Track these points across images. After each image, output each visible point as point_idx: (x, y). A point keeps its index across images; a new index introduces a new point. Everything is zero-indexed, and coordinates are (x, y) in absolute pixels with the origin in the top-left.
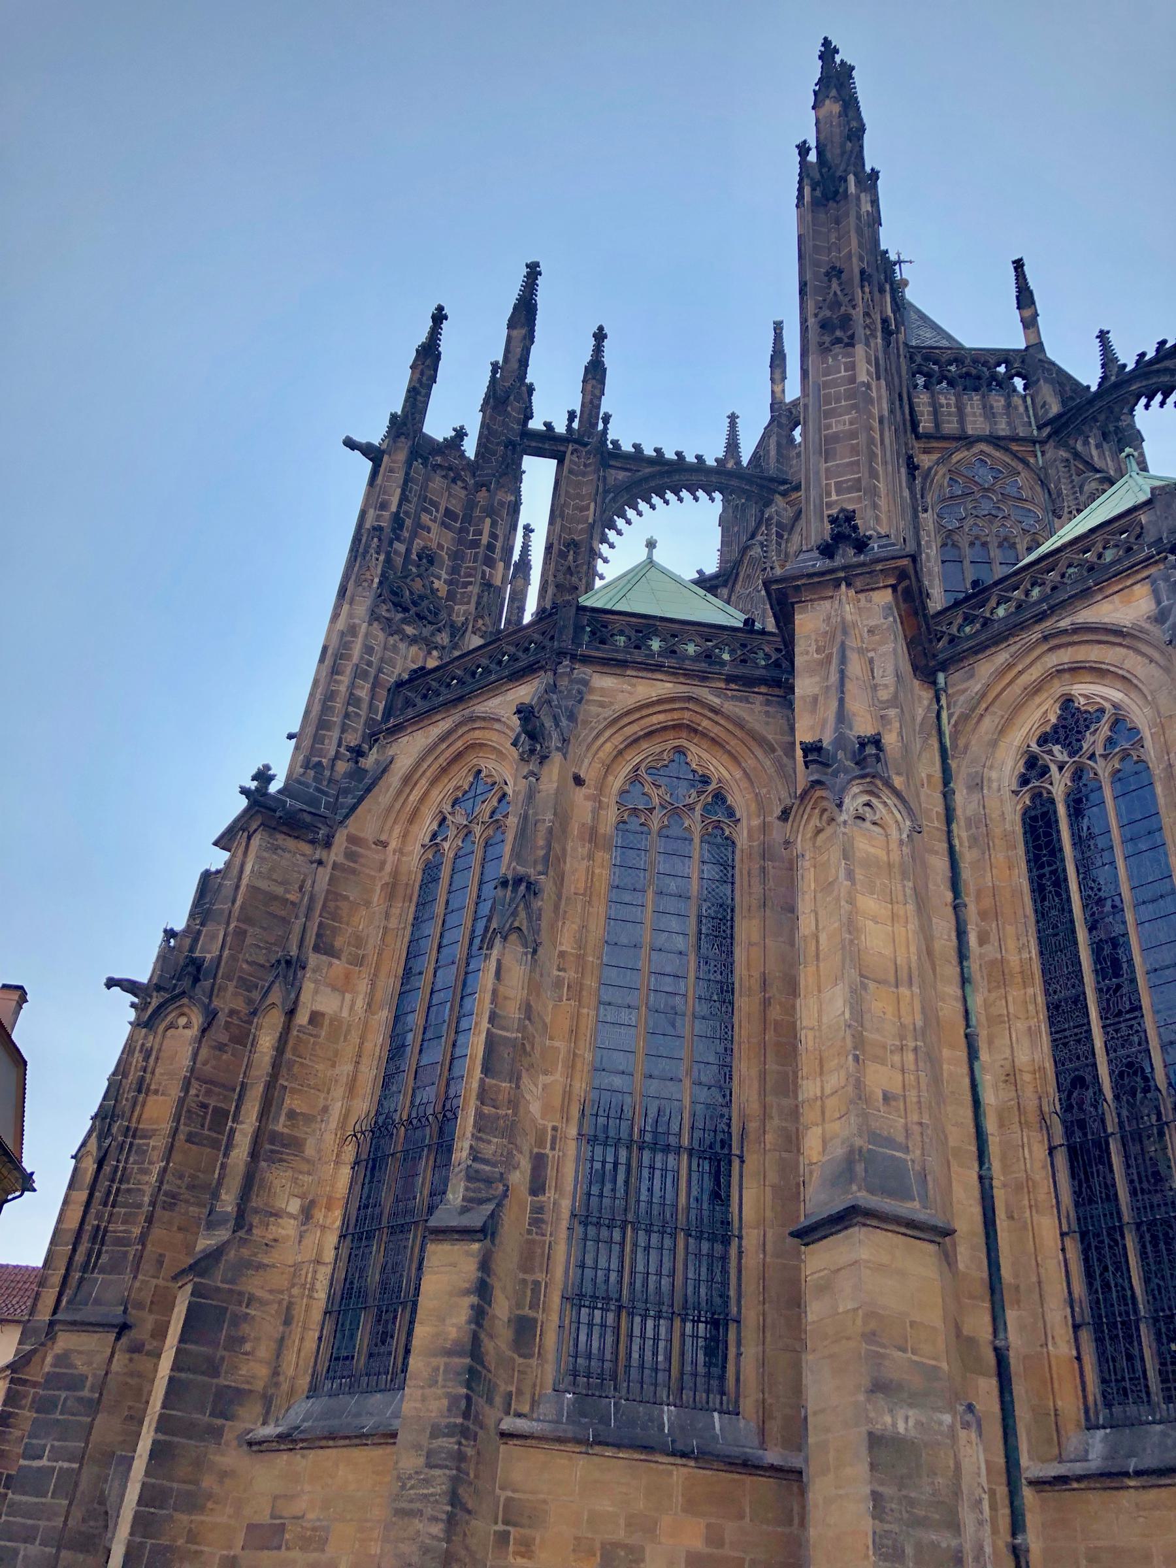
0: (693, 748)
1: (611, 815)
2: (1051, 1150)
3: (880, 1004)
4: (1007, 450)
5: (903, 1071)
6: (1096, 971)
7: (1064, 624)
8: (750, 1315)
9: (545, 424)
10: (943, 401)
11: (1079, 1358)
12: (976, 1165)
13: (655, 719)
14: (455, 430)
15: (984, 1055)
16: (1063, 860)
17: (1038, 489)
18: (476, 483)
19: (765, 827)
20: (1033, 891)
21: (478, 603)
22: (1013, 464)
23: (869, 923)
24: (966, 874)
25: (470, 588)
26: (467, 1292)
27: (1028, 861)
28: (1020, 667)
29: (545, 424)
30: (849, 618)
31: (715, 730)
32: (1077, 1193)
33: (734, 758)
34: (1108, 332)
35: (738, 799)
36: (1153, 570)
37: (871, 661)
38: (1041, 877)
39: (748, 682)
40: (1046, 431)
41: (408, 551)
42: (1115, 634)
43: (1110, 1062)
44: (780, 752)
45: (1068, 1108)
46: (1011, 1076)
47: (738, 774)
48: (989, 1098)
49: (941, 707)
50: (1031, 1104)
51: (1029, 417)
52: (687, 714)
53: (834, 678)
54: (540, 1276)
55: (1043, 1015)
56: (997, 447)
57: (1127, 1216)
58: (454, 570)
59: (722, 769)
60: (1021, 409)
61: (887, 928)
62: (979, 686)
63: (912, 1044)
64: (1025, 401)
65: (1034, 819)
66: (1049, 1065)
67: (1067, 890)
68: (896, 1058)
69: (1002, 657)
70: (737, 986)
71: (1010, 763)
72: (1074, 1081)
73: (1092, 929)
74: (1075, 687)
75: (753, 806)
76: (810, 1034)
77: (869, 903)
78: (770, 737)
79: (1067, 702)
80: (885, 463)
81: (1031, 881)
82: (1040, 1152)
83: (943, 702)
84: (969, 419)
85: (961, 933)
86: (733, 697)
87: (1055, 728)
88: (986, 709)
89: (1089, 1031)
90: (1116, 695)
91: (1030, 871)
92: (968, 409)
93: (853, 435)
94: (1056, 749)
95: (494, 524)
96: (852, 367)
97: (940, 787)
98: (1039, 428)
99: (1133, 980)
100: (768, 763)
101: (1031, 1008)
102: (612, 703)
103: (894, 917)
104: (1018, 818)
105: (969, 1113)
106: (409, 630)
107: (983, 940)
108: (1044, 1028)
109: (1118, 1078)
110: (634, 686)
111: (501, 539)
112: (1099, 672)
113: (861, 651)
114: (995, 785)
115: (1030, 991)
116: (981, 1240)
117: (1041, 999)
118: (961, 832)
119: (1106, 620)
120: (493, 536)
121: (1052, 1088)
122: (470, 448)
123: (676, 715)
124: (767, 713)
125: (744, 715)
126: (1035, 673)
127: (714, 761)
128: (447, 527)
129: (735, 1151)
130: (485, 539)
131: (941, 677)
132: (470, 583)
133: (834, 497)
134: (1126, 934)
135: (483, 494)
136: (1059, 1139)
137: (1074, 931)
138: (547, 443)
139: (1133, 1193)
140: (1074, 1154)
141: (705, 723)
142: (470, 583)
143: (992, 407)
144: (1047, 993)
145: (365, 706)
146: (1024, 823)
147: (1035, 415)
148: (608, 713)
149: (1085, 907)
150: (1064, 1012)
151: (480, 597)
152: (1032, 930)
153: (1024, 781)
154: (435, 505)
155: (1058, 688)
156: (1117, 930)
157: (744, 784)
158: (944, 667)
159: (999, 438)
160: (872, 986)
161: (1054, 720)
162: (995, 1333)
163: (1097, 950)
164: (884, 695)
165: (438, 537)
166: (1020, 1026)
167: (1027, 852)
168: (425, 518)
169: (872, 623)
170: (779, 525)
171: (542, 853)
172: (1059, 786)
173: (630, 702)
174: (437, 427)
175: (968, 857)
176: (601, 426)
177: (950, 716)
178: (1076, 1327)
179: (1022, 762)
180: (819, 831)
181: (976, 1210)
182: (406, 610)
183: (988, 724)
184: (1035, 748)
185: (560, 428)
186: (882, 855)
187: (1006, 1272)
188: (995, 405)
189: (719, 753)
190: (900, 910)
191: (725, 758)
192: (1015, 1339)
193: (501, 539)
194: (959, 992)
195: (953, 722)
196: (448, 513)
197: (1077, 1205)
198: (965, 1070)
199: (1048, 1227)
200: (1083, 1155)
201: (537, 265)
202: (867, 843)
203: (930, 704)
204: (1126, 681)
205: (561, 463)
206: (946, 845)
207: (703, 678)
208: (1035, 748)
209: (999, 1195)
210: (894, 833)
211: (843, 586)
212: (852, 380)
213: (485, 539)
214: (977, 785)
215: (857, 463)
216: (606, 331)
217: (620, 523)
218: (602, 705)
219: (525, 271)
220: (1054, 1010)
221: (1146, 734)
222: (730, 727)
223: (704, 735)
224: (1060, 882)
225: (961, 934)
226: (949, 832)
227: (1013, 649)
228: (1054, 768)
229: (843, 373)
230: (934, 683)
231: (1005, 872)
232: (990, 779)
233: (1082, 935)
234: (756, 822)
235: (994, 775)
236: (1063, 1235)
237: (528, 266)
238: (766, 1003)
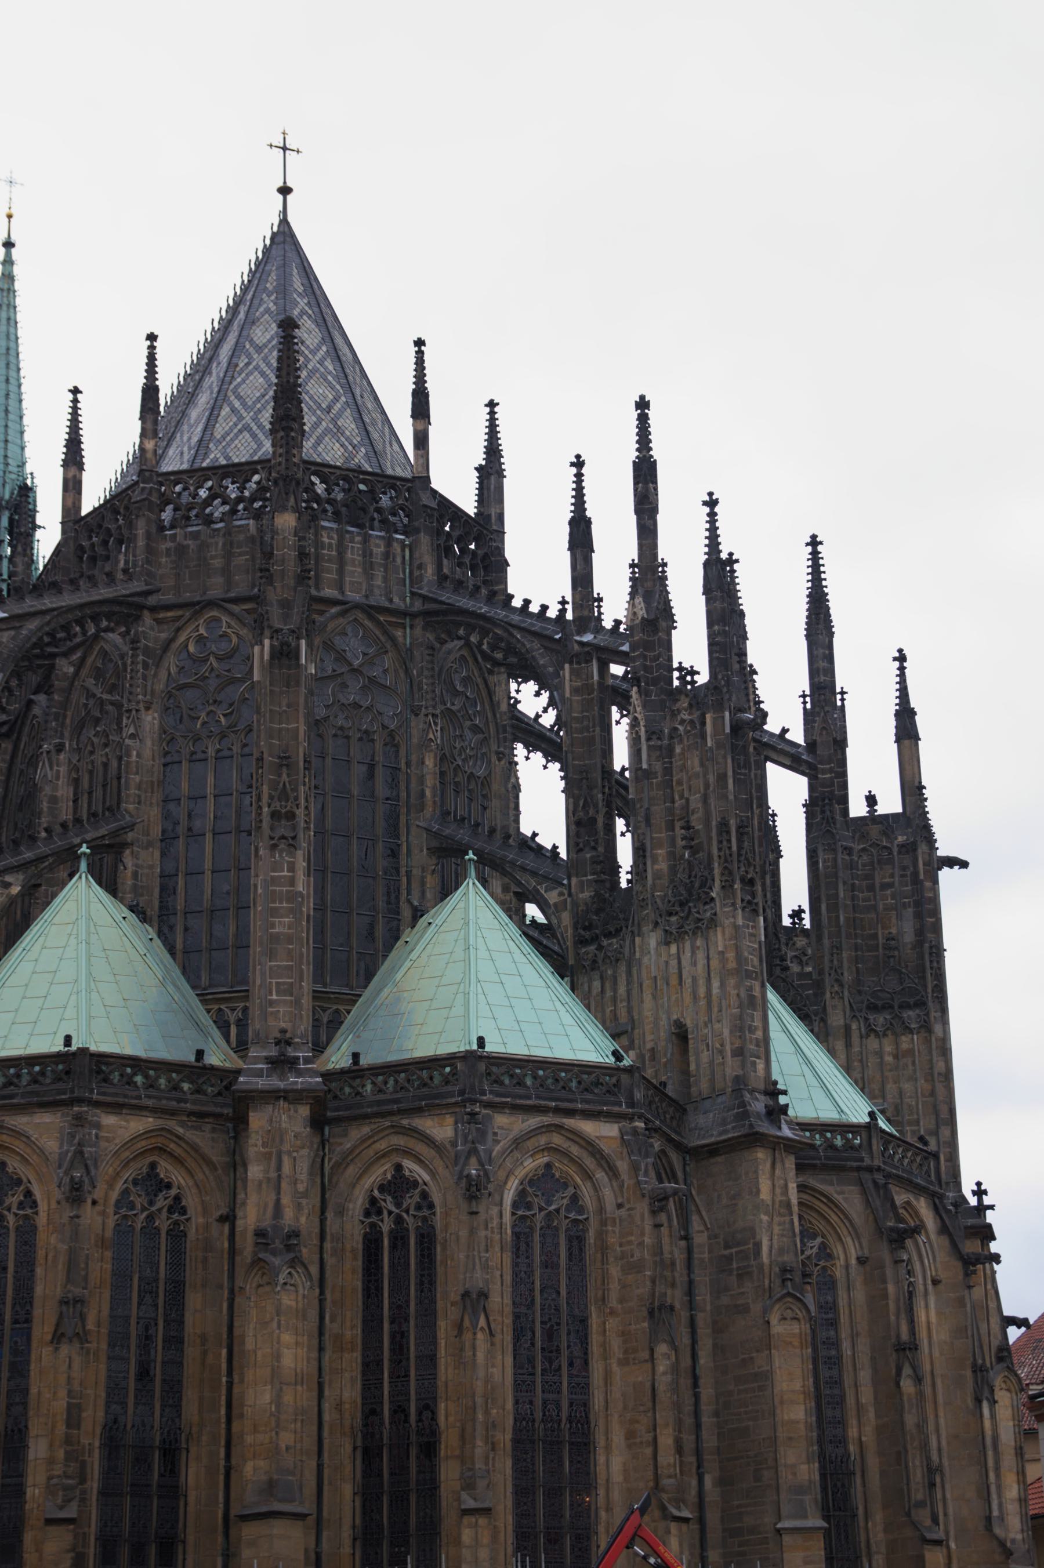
0: (163, 1163)
1: (111, 1222)
2: (355, 1449)
3: (288, 1398)
4: (379, 623)
5: (295, 1432)
6: (391, 1350)
7: (405, 1122)
8: (191, 1539)
10: (326, 540)
11: (354, 1554)
12: (316, 1457)
13: (139, 1145)
15: (327, 1393)
16: (382, 1274)
17: (402, 675)
19: (207, 1227)
20: (364, 1290)
22: (382, 638)
23: (285, 1350)
24: (328, 1273)
26: (68, 1551)
27: (364, 1269)
28: (376, 1138)
30: (284, 1125)
31: (178, 1151)
32: (364, 1472)
34: (498, 404)
35: (191, 1201)
36: (457, 1110)
37: (295, 1158)
38: (369, 1281)
39: (201, 1115)
40: (418, 605)
42: (429, 1141)
43: (390, 1402)
44: (220, 1171)
45: (365, 1425)
46: (339, 1406)
47: (191, 1183)
48: (326, 1417)
49: (325, 1154)
50: (347, 1422)
51: (404, 573)
52: (160, 1139)
53: (273, 1175)
54: (86, 1530)
55: (360, 1368)
56: (371, 617)
57: (386, 1488)
59: (180, 1178)
60: (399, 560)
61: (293, 1353)
62: (349, 1146)
63: (300, 1418)
64: (403, 551)
66: (359, 1400)
67: (382, 1295)
68: (293, 1426)
69: (366, 1130)
70: (186, 1339)
71: (360, 1202)
72: (371, 1412)
73: (392, 1322)
74: (405, 1161)
75: (199, 1208)
76: (250, 1410)
77: (287, 1338)
78: (214, 1159)
79: (399, 1168)
80: (308, 964)
81: (363, 1283)
82: (348, 1448)
83: (327, 1150)
84: (349, 568)
85: (322, 1318)
86: (192, 1126)
87: (389, 1182)
88: (352, 1160)
89: (382, 1383)
90: (426, 1177)
91: (364, 1276)
92: (349, 555)
93: (289, 939)
94: (389, 1199)
96: (292, 868)
97: (319, 1213)
98: (413, 594)
99: (408, 1359)
100: (211, 1178)
101: (354, 1365)
102: (114, 1138)
103: (297, 1343)
104: (361, 1239)
105: (315, 1428)
107: (332, 1321)
108: (359, 1377)
109: (394, 1412)
110: (127, 1121)
112: (419, 1161)
113: (289, 1153)
114: (350, 1213)
115: (355, 1354)
116: (314, 1498)
117: (359, 1360)
118: (328, 1245)
119: (428, 1131)
121: (359, 1415)
123: (153, 1140)
124: (213, 1139)
125: (198, 1141)
126: (382, 1145)
127: (176, 1172)
129: (184, 1445)
131: (327, 1129)
133: (274, 997)
134: (408, 1331)
136: (359, 1443)
137: (382, 1322)
139: (391, 1474)
140: (366, 1451)
141: (172, 1146)
143: (371, 555)
144: (363, 1355)
146: (364, 1243)
147: (411, 573)
148: (113, 1148)
149: (390, 1308)
150: (370, 1368)
152: (360, 1315)
153: (367, 1214)
155: (396, 1159)
156: (404, 1329)
157: (194, 1191)
158: (330, 1122)
159: (371, 607)
160: (284, 1387)
161: (389, 1176)
162: (317, 1545)
163: (393, 1337)
164: (301, 1188)
166: (347, 1375)
167: (363, 1262)
169: (297, 1129)
171: (83, 1273)
172: (386, 1226)
173: (127, 1135)
175: (330, 1261)
177: (330, 1159)
178: (355, 1539)
180: (259, 1286)
181: (313, 1483)
183: (351, 1171)
184: (376, 1193)
186: (294, 1304)
187: (325, 1514)
188: (375, 550)
190: (300, 1339)
192: (325, 1546)
194: (317, 1355)
195: (331, 1164)
197: (363, 1477)
198: (315, 1403)
199: (348, 1490)
200: (369, 1453)
202: (288, 1300)
203: (318, 1150)
204: (433, 1174)
206: (318, 1256)
207: (172, 1113)
208: (376, 1193)
209: (326, 1472)
210: (301, 1291)
211: (282, 1102)
212: (292, 882)
214: (341, 1212)
215: (290, 968)
218: (108, 1140)
220: (366, 1365)
221: (438, 1210)
222: (189, 1149)
223: (171, 1155)
224: (379, 1289)
225: (322, 1318)
226: (321, 1248)
227: (373, 1127)
228: (385, 1213)
229: (285, 873)
230: (323, 1134)
231: (348, 1275)
233: (386, 1326)
234: (201, 1220)
235: (351, 1206)
236: (355, 1494)
238: (205, 1353)
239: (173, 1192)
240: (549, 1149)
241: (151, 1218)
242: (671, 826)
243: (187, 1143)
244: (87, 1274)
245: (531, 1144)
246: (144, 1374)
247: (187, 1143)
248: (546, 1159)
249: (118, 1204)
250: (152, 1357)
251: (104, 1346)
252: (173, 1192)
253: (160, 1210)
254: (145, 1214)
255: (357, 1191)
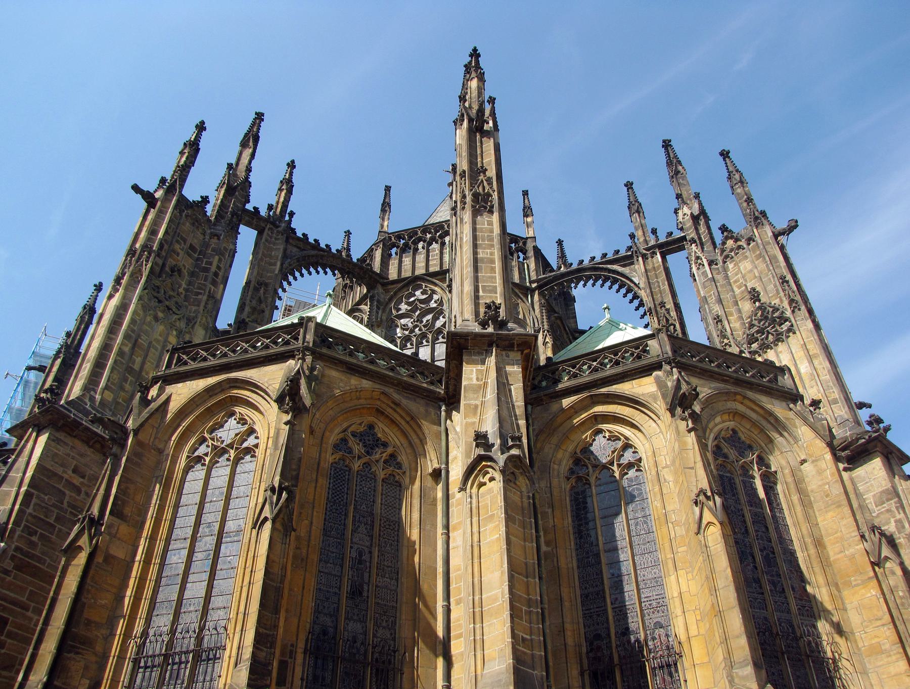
0: (381, 425)
1: (330, 458)
9: (254, 208)
14: (202, 197)
18: (211, 233)
21: (205, 307)
25: (200, 297)
29: (254, 208)
33: (405, 434)
38: (580, 525)
41: (164, 265)
47: (406, 444)
52: (378, 403)
58: (190, 283)
65: (577, 493)
95: (220, 260)
106: (160, 315)
111: (222, 271)
120: (219, 268)
122: (210, 210)
128: (189, 255)
130: (213, 268)
132: (201, 294)
135: (215, 240)
138: (254, 219)
141: (389, 410)
142: (201, 294)
145: (127, 357)
151: (206, 303)
153: (572, 471)
154: (185, 241)
165: (185, 262)
168: (177, 247)
170: (378, 301)
174: (192, 191)
176: (287, 218)
177: (533, 430)
179: (571, 462)
182: (160, 301)
184: (579, 455)
185: (263, 212)
189: (396, 429)
191: (398, 433)
193: (222, 271)
196: (192, 247)
201: (263, 114)
205: (260, 234)
213: (213, 268)
216: (296, 164)
217: (291, 278)
219: (254, 116)
232: (554, 469)
235: (556, 467)
237: (256, 113)
239: (390, 450)
240: (735, 414)
241: (367, 465)
242: (736, 303)
243: (403, 409)
244: (298, 475)
245: (721, 406)
246: (356, 592)
247: (403, 409)
248: (731, 424)
249: (336, 447)
250: (366, 580)
251: (314, 557)
252: (390, 450)
253: (377, 461)
254: (363, 460)
255: (560, 455)
